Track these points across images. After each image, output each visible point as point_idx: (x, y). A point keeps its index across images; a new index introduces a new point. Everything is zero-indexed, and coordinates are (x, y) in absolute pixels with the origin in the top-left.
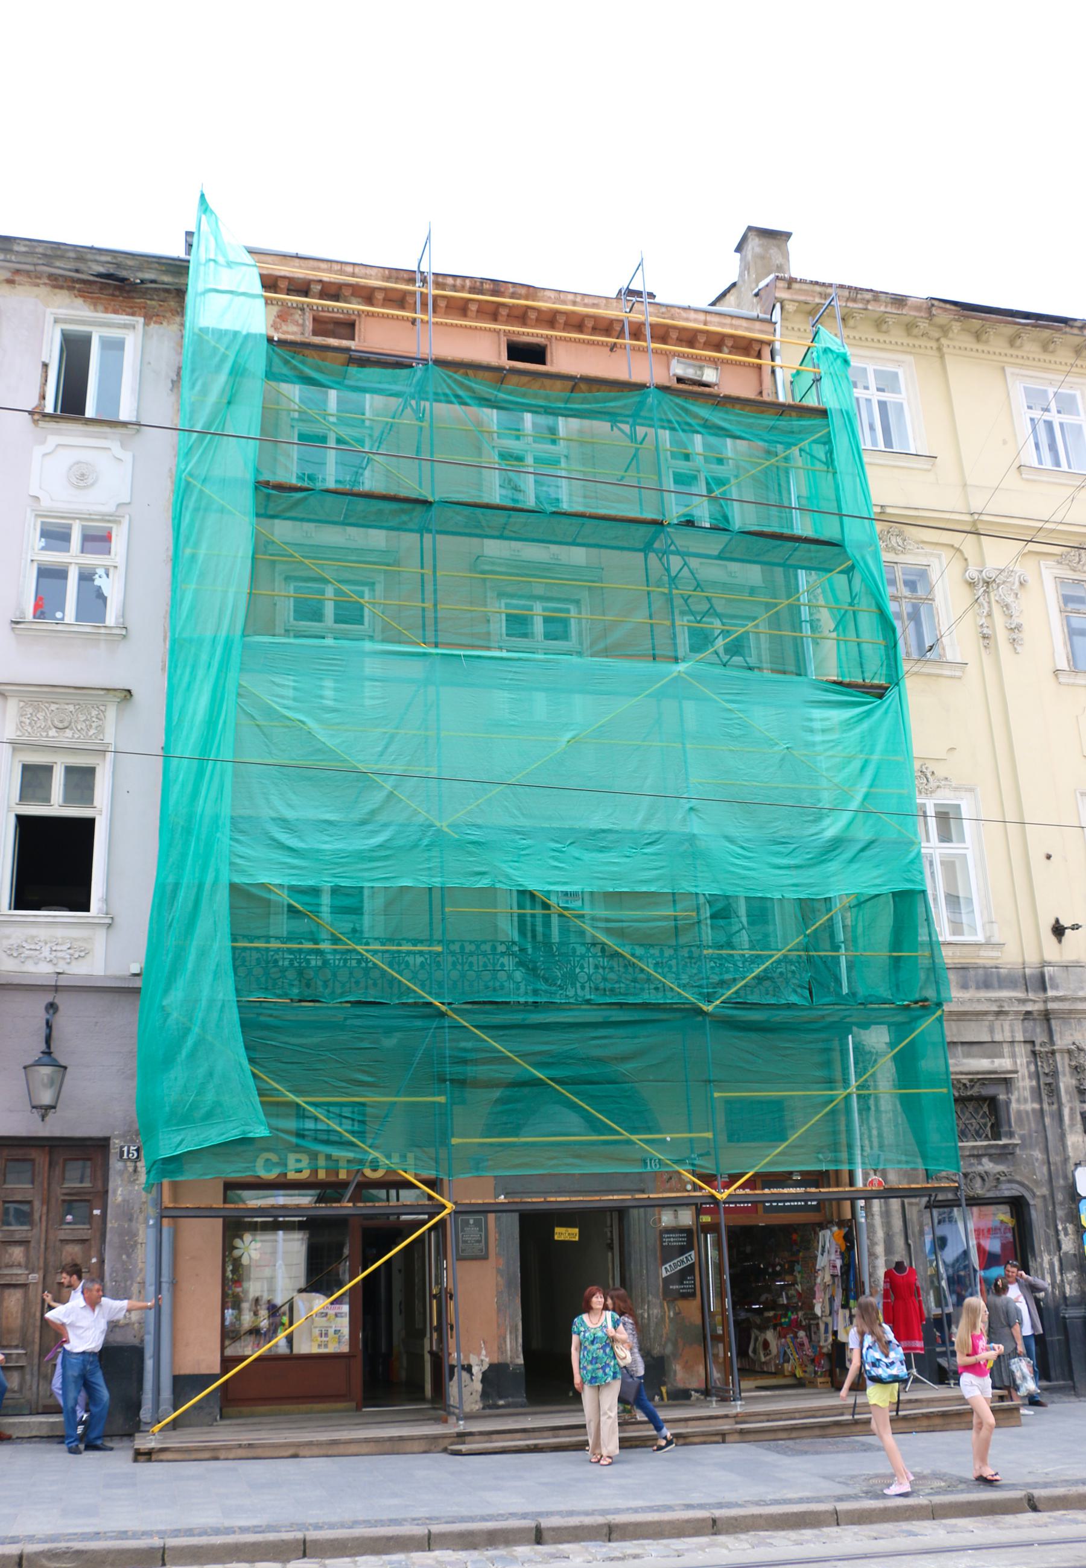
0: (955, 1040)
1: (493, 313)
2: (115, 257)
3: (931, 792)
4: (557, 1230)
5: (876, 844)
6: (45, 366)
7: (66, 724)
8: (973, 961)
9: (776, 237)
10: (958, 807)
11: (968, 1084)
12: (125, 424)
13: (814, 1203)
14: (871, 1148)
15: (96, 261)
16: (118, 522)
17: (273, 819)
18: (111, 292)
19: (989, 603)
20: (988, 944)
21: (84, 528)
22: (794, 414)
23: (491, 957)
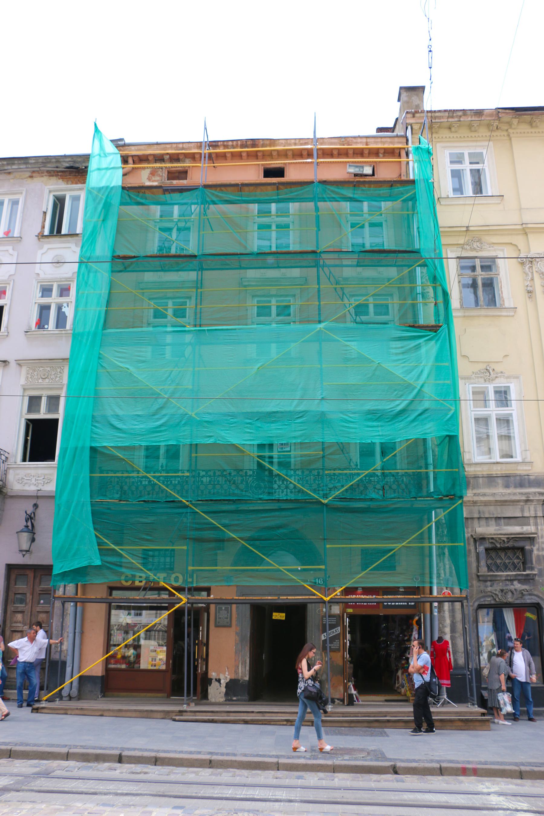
0: (499, 516)
1: (255, 156)
2: (72, 158)
3: (492, 380)
4: (274, 614)
5: (427, 412)
6: (45, 213)
7: (46, 376)
8: (514, 472)
9: (418, 90)
10: (509, 387)
11: (506, 540)
12: (78, 234)
13: (413, 604)
14: (445, 574)
15: (64, 161)
16: (73, 281)
17: (112, 415)
18: (74, 174)
19: (532, 273)
20: (524, 463)
21: (59, 286)
22: (398, 185)
23: (213, 477)
